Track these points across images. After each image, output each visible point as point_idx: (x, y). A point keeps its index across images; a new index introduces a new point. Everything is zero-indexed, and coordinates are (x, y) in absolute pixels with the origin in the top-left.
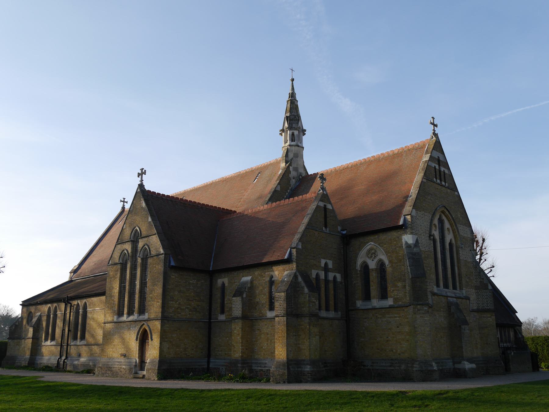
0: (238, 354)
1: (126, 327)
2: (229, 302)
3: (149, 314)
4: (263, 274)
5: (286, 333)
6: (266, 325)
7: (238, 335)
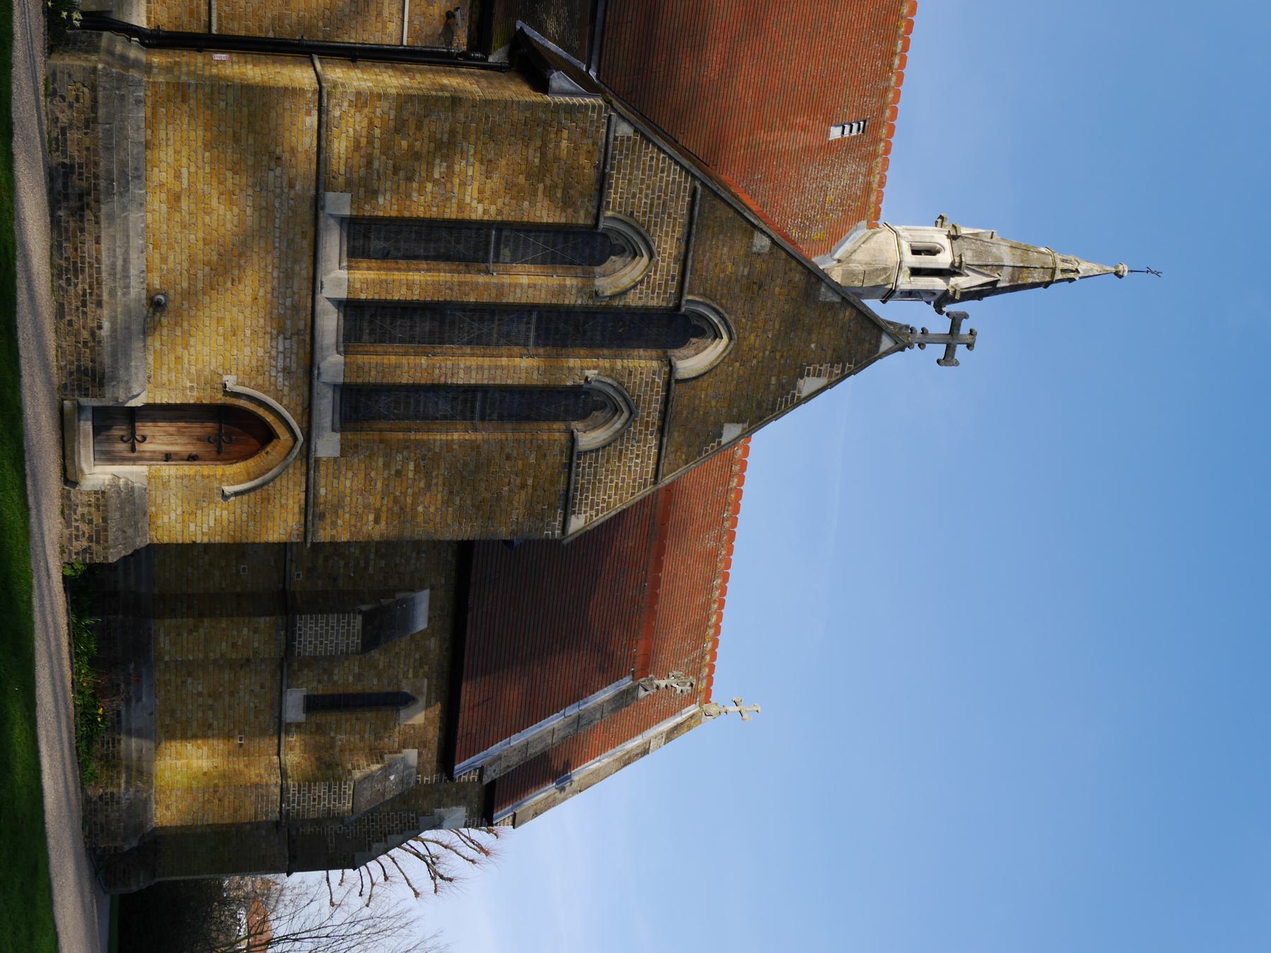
0: (167, 648)
3: (335, 459)
4: (426, 668)
5: (230, 821)
6: (262, 687)
7: (234, 645)
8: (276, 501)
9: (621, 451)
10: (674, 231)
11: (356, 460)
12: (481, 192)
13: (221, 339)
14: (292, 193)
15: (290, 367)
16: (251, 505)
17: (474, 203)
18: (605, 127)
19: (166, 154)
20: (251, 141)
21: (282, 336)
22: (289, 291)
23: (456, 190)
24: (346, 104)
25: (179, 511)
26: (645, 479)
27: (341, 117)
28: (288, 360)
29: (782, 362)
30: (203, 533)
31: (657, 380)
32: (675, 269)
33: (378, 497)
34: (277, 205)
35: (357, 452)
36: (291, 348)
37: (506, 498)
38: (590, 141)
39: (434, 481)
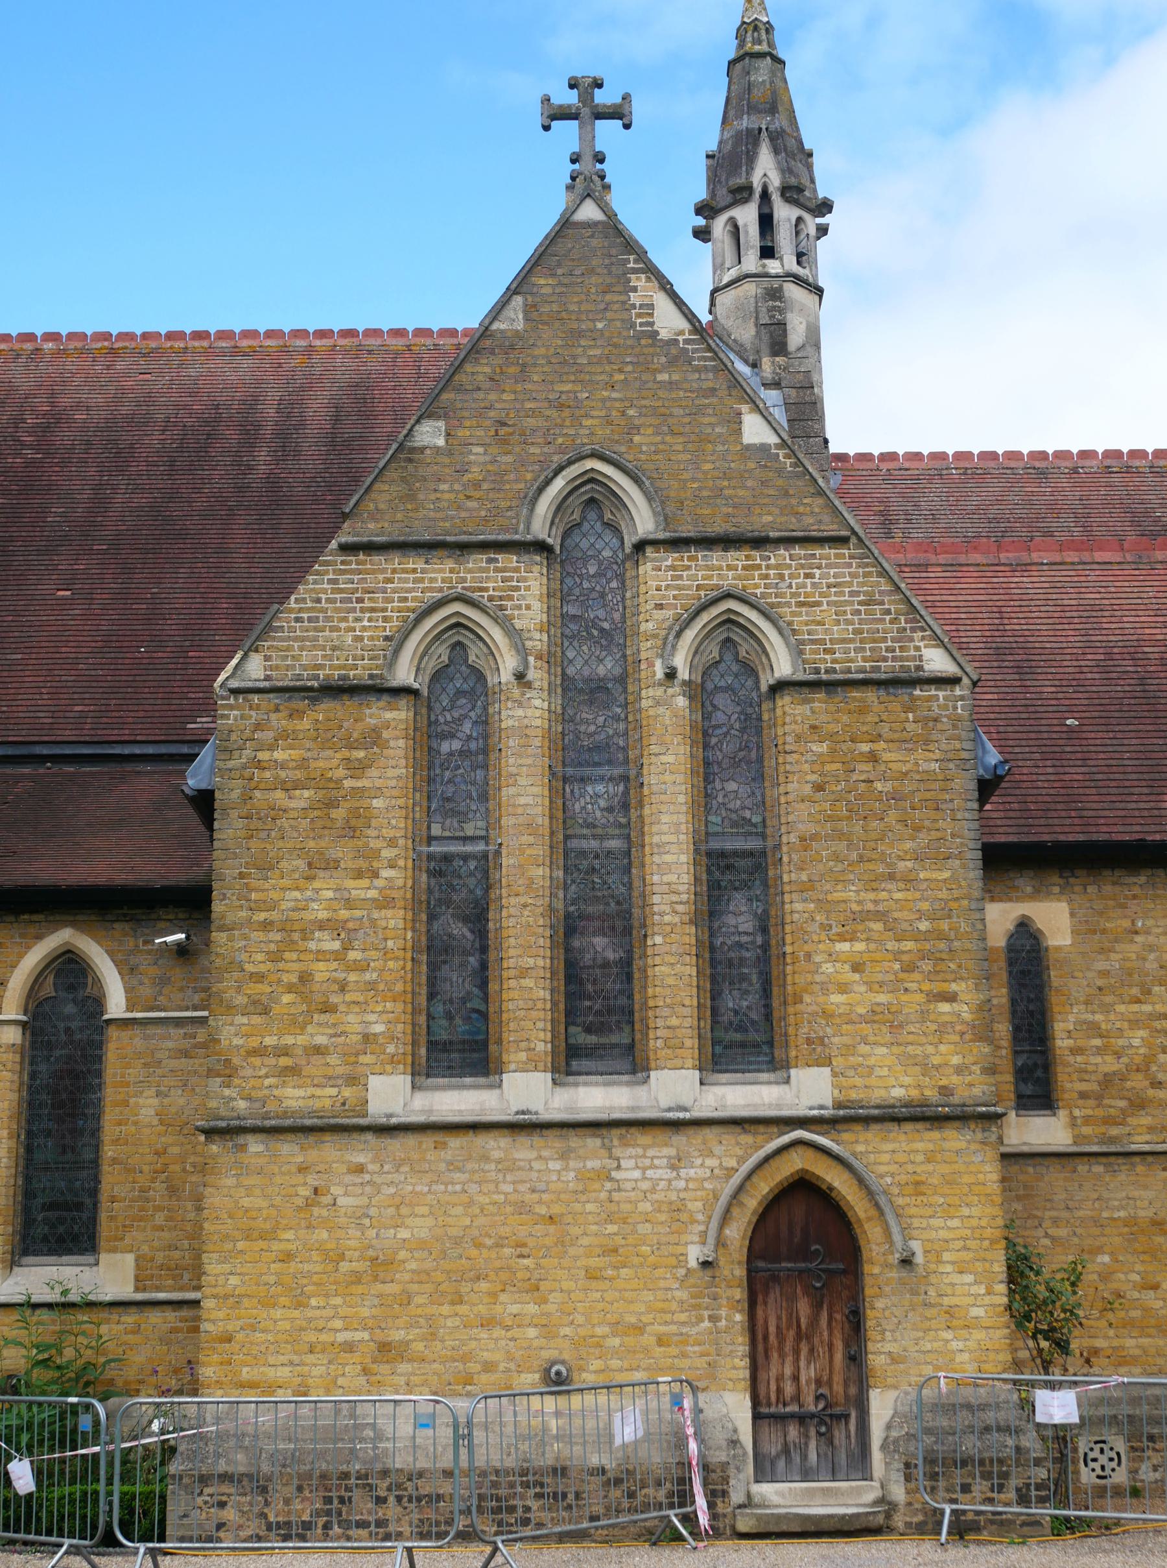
1: (555, 1165)
2: (1097, 1042)
3: (835, 1074)
8: (919, 1170)
9: (801, 604)
10: (414, 571)
11: (836, 1040)
12: (359, 874)
13: (624, 1271)
14: (371, 1167)
15: (669, 1158)
16: (930, 1212)
17: (379, 883)
18: (251, 696)
19: (315, 1365)
20: (289, 1235)
21: (614, 1174)
22: (536, 1165)
23: (358, 913)
24: (227, 1092)
25: (948, 1335)
26: (851, 557)
27: (249, 1098)
28: (656, 1162)
29: (629, 368)
30: (989, 1292)
31: (669, 563)
32: (477, 560)
33: (905, 998)
34: (392, 1190)
35: (821, 1039)
36: (637, 1157)
37: (896, 783)
38: (273, 716)
39: (870, 906)
